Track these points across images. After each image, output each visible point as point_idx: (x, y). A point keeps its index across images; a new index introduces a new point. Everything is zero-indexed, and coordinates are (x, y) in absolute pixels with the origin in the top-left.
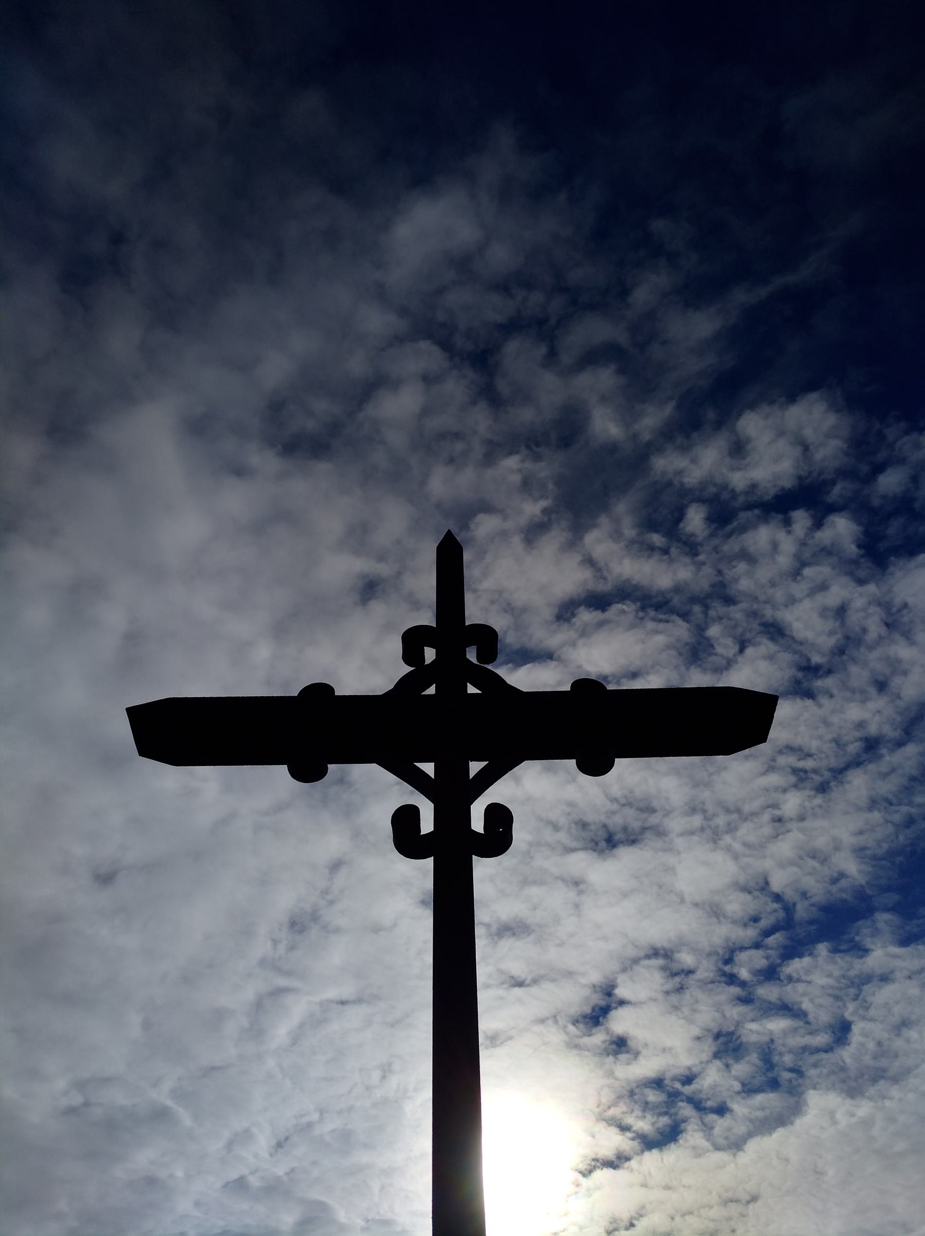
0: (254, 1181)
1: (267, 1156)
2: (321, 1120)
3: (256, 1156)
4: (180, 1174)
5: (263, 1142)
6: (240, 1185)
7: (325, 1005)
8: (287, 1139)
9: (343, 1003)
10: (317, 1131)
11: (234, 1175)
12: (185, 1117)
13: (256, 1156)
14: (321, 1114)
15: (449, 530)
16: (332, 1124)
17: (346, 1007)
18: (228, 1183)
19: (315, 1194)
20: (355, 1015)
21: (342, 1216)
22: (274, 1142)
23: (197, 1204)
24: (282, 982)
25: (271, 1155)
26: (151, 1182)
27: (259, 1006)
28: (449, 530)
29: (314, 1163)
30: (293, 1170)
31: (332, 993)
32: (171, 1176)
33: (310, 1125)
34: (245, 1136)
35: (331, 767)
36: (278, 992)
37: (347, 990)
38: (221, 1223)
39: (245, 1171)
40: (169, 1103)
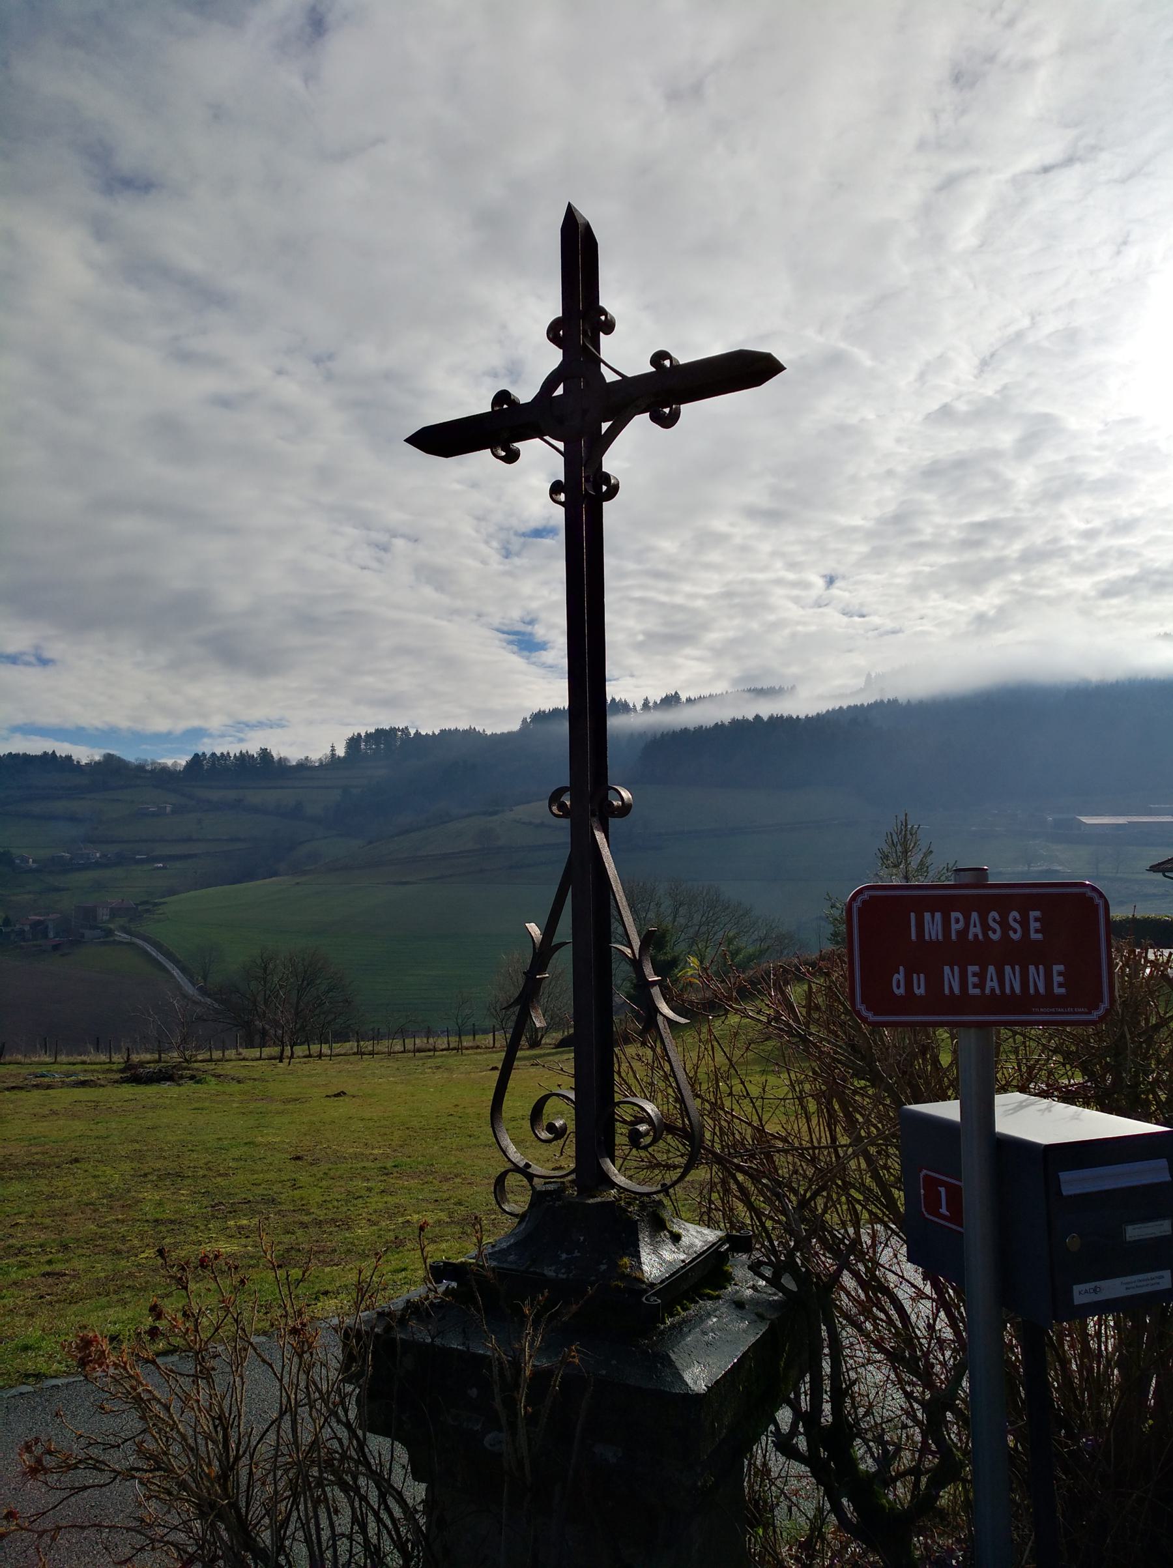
0: (962, 407)
1: (971, 378)
2: (1034, 324)
3: (957, 381)
4: (871, 416)
5: (964, 366)
6: (945, 413)
7: (1018, 182)
8: (992, 355)
9: (1046, 170)
10: (1030, 339)
11: (934, 406)
12: (864, 358)
13: (957, 381)
14: (1033, 318)
15: (785, 369)
16: (1051, 325)
17: (1051, 175)
18: (930, 414)
19: (1037, 407)
20: (1069, 181)
21: (1073, 423)
22: (976, 361)
23: (899, 441)
24: (955, 164)
25: (976, 377)
26: (843, 430)
27: (927, 211)
28: (785, 369)
29: (1030, 375)
30: (1005, 387)
31: (1030, 160)
32: (863, 420)
33: (1019, 335)
34: (942, 363)
35: (424, 1486)
36: (950, 183)
37: (1052, 152)
38: (929, 454)
39: (947, 399)
40: (842, 345)
